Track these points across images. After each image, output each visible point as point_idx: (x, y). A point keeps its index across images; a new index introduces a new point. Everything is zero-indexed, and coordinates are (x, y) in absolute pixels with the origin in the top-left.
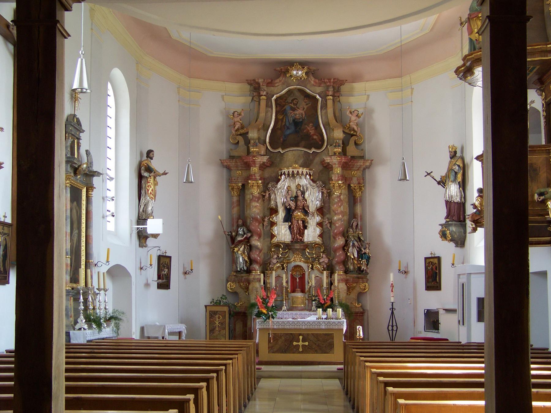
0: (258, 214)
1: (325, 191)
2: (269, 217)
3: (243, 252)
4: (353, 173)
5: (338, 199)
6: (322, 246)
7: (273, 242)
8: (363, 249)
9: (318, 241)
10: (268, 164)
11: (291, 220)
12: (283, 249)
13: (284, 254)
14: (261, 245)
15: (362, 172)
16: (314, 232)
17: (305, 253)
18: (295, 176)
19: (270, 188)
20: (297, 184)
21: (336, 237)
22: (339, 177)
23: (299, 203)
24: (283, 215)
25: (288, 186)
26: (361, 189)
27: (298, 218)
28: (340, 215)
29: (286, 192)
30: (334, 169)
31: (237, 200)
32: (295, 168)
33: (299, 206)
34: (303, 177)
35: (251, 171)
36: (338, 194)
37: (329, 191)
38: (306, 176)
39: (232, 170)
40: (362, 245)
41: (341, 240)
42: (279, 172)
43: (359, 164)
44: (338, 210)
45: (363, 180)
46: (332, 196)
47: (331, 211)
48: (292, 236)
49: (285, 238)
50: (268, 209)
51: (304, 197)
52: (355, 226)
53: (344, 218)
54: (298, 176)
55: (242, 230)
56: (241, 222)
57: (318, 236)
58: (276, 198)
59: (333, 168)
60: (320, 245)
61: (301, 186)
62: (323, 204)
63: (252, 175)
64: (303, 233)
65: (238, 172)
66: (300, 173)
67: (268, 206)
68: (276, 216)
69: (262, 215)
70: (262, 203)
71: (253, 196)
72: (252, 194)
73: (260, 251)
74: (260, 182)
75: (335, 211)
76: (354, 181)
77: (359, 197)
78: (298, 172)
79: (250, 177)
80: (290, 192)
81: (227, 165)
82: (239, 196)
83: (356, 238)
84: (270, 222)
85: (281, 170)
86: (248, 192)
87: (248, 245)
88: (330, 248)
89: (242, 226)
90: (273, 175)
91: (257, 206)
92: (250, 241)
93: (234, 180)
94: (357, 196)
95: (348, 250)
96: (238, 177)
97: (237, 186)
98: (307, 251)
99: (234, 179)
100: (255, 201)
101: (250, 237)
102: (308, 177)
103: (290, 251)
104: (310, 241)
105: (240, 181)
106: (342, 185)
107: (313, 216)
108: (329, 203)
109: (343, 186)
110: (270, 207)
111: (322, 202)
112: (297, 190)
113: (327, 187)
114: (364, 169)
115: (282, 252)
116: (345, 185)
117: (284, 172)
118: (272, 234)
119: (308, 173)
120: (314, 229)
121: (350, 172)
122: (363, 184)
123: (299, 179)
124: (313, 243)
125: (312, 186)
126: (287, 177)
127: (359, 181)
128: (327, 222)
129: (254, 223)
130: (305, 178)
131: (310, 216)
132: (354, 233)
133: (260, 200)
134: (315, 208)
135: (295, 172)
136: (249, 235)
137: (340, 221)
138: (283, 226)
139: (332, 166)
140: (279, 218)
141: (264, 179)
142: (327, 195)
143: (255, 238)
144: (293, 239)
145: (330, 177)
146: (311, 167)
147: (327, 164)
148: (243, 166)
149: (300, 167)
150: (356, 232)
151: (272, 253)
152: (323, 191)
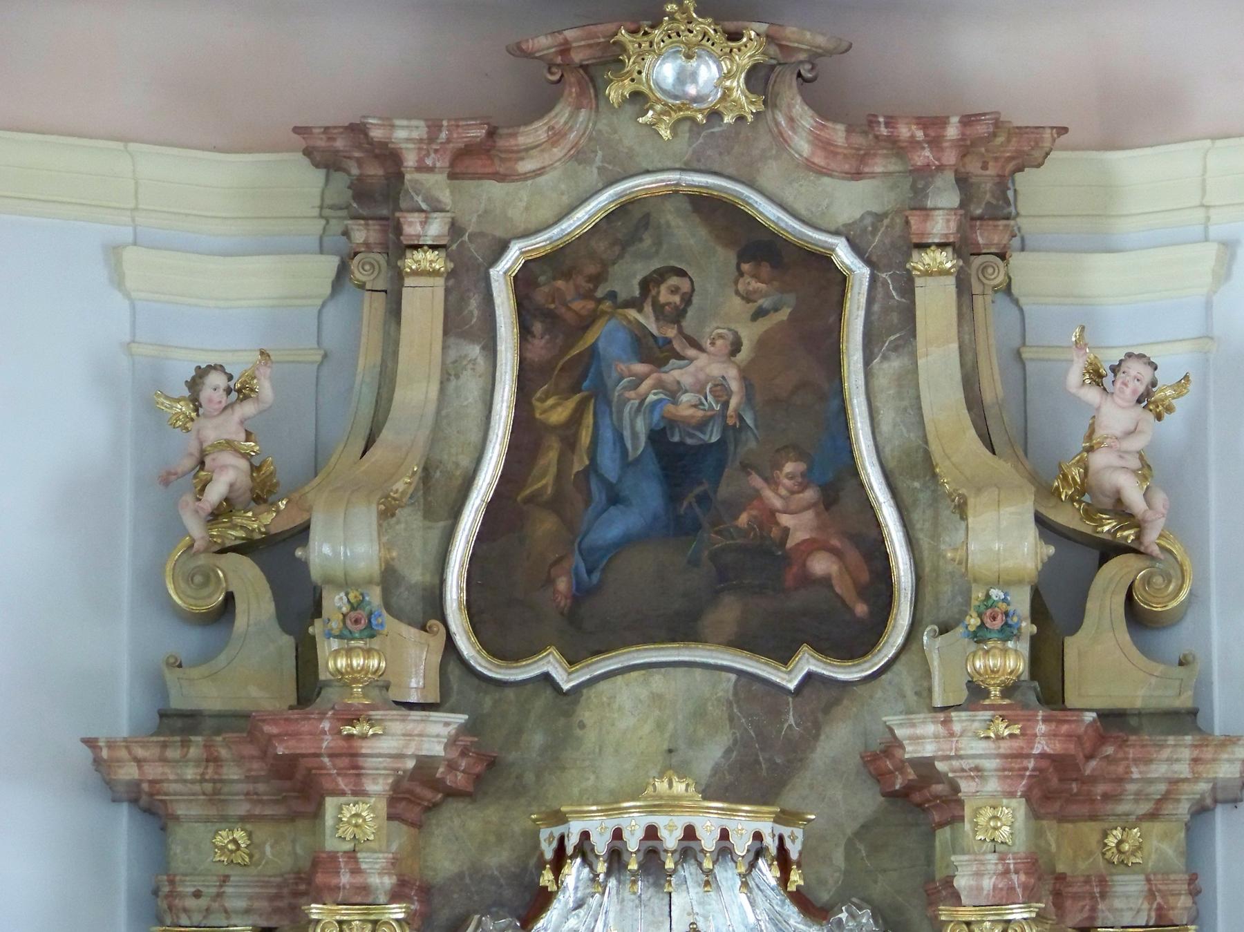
4: (1111, 841)
10: (460, 776)
15: (1183, 835)
18: (669, 865)
22: (1006, 872)
30: (968, 811)
32: (669, 805)
34: (728, 876)
35: (328, 832)
38: (752, 865)
39: (176, 818)
42: (544, 833)
43: (1159, 770)
45: (1195, 893)
54: (689, 871)
59: (960, 803)
63: (333, 857)
65: (223, 838)
66: (708, 841)
74: (397, 912)
76: (1118, 904)
79: (320, 879)
81: (137, 784)
85: (559, 818)
90: (498, 859)
93: (191, 903)
96: (225, 879)
99: (197, 895)
102: (768, 873)
105: (242, 904)
114: (1202, 811)
117: (585, 835)
119: (771, 844)
121: (1090, 831)
123: (695, 892)
126: (609, 874)
127: (1159, 900)
130: (745, 884)
135: (671, 839)
139: (956, 789)
141: (426, 892)
145: (939, 875)
146: (790, 800)
147: (911, 775)
148: (261, 787)
149: (705, 798)
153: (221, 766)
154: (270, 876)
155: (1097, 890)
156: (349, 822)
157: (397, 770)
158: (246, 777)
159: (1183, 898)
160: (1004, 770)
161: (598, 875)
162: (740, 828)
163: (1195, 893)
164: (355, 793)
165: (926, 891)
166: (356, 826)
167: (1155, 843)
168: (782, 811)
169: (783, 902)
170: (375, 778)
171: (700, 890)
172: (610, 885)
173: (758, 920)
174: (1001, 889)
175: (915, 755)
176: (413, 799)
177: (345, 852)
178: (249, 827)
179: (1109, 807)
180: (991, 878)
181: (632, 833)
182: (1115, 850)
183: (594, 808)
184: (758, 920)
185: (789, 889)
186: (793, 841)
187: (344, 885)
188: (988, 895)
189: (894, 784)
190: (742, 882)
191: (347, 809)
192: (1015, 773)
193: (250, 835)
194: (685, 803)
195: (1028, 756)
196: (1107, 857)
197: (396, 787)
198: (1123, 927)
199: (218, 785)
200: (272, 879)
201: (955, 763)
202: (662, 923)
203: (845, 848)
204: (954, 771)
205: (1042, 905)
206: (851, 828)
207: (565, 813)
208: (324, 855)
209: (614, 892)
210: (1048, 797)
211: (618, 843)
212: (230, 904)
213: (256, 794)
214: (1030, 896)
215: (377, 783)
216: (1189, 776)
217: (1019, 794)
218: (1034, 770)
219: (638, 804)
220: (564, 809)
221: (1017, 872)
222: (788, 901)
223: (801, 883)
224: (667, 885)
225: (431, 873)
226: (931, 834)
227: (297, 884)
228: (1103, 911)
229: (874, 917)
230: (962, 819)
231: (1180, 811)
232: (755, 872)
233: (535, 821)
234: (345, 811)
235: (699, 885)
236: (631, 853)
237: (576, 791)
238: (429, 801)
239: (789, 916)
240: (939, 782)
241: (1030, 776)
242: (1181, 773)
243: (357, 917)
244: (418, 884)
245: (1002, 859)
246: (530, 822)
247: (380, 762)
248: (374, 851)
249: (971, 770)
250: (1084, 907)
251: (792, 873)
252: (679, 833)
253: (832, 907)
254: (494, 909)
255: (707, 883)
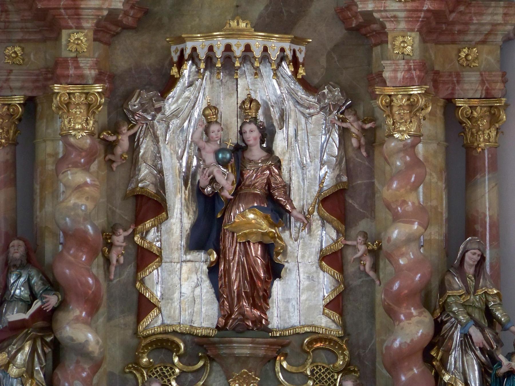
0: (87, 218)
1: (355, 124)
2: (131, 231)
3: (27, 371)
4: (463, 55)
5: (408, 158)
6: (341, 347)
7: (145, 329)
8: (502, 357)
9: (323, 325)
10: (130, 19)
11: (218, 240)
12: (185, 360)
13: (190, 377)
14: (98, 343)
15: (499, 52)
16: (309, 288)
17: (271, 374)
18: (237, 64)
19: (134, 113)
20: (242, 96)
21: (396, 308)
22: (409, 70)
23: (249, 173)
24: (188, 223)
25: (209, 107)
26: (494, 119)
27: (245, 234)
28: (412, 223)
29: (201, 129)
30: (390, 38)
31: (7, 161)
32: (238, 34)
33: (249, 186)
35: (63, 47)
36: (406, 136)
37: (368, 126)
38: (279, 65)
40: (498, 341)
41: (418, 322)
42: (173, 48)
43: (487, 19)
44: (404, 202)
45: (505, 82)
46: (382, 144)
47: (379, 206)
48: (221, 306)
49: (192, 314)
50: (125, 197)
51: (269, 150)
52: (471, 266)
53: (430, 234)
54: (247, 68)
55: (22, 280)
56: (22, 249)
57: (327, 306)
58: (159, 152)
59: (386, 34)
60: (330, 340)
61: (258, 106)
62: (345, 179)
63: (66, 60)
64: (267, 296)
65: (9, 51)
66: (257, 53)
67: (127, 188)
68: (158, 225)
69: (101, 221)
70: (103, 173)
71: (68, 145)
72: (65, 137)
73: (97, 366)
74: (98, 88)
75: (394, 206)
76: (466, 86)
77: (488, 150)
78: (248, 48)
79: (59, 71)
80: (214, 128)
82: (14, 144)
83: (477, 315)
84: (133, 251)
85: (181, 40)
86: (49, 131)
87: (49, 339)
88: (373, 352)
89: (22, 267)
91: (86, 184)
92: (55, 326)
94: (482, 145)
95: (444, 362)
96: (10, 72)
97: (4, 105)
98: (281, 366)
100: (76, 165)
101: (54, 310)
102: (287, 69)
103: (215, 364)
104: (293, 327)
105: (18, 84)
106: (422, 102)
107: (305, 226)
108: (371, 172)
109: (426, 107)
110: (133, 190)
111: (340, 171)
112: (244, 123)
113: (361, 111)
115: (182, 372)
116: (434, 102)
117: (194, 49)
118: (141, 296)
119: (289, 53)
120: (310, 278)
121: (452, 49)
122: (504, 100)
123: (249, 79)
124: (307, 333)
125: (302, 105)
126: (205, 69)
127: (487, 85)
128: (362, 248)
129: (71, 252)
130: (275, 75)
131: (293, 225)
132: (468, 292)
133: (96, 162)
134: (315, 194)
135: (238, 51)
136: (53, 300)
137: (414, 246)
138: (186, 267)
139: (383, 27)
140: (170, 232)
142: (363, 141)
143: (77, 312)
144: (227, 317)
145: (375, 71)
146: (299, 32)
147: (361, 20)
148: (29, 25)
149: (255, 31)
150: (476, 288)
151: (142, 375)
152: (344, 125)
153: (9, 14)
154: (34, 70)
155: (455, 79)
156: (74, 43)
157: (98, 16)
158: (22, 20)
159: (499, 84)
160: (408, 17)
161: (200, 70)
162: (273, 46)
163: (505, 82)
164: (77, 28)
165: (368, 79)
166: (78, 44)
167: (485, 56)
168: (295, 37)
169: (295, 83)
170: (87, 20)
171: (253, 77)
172: (206, 74)
173: (282, 93)
174: (407, 78)
175: (363, 10)
176: (106, 30)
177: (72, 58)
178: (22, 45)
179: (461, 37)
180: (401, 73)
181: (218, 48)
182: (464, 59)
183: (199, 35)
184: (282, 93)
185: (298, 77)
186: (300, 53)
187: (71, 75)
188: (400, 81)
189: (352, 24)
190: (274, 73)
191: (73, 36)
192: (414, 19)
193: (23, 49)
194: (245, 33)
195: (421, 11)
196: (460, 62)
197: (97, 25)
198: (468, 99)
199: (7, 24)
200: (35, 72)
201: (384, 14)
202: (233, 94)
203: (327, 55)
204: (383, 18)
205: (428, 87)
206: (329, 46)
207: (184, 38)
208: (61, 59)
209: (208, 78)
210: (430, 32)
211: (211, 53)
212: (12, 84)
213: (26, 28)
214: (421, 83)
215: (88, 23)
216: (502, 22)
217: (416, 30)
218: (423, 18)
219: (222, 33)
220: (183, 36)
221: (415, 70)
222: (297, 83)
223: (304, 74)
224: (235, 75)
225: (115, 68)
226: (370, 51)
227: (46, 74)
228: (458, 90)
229: (341, 91)
230: (387, 42)
231: (498, 40)
232: (281, 68)
233: (168, 42)
234: (72, 37)
235: (252, 75)
236: (218, 58)
237: (189, 26)
238: (114, 31)
239: (298, 91)
240: (374, 24)
241: (422, 21)
242: (498, 20)
243: (77, 91)
244: (108, 73)
245: (407, 63)
246: (166, 43)
247: (90, 12)
248: (86, 57)
249: (391, 17)
250: (449, 87)
251: (300, 69)
252: (242, 48)
253: (320, 86)
254: (147, 87)
255: (256, 74)
